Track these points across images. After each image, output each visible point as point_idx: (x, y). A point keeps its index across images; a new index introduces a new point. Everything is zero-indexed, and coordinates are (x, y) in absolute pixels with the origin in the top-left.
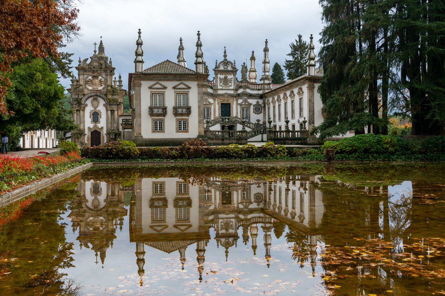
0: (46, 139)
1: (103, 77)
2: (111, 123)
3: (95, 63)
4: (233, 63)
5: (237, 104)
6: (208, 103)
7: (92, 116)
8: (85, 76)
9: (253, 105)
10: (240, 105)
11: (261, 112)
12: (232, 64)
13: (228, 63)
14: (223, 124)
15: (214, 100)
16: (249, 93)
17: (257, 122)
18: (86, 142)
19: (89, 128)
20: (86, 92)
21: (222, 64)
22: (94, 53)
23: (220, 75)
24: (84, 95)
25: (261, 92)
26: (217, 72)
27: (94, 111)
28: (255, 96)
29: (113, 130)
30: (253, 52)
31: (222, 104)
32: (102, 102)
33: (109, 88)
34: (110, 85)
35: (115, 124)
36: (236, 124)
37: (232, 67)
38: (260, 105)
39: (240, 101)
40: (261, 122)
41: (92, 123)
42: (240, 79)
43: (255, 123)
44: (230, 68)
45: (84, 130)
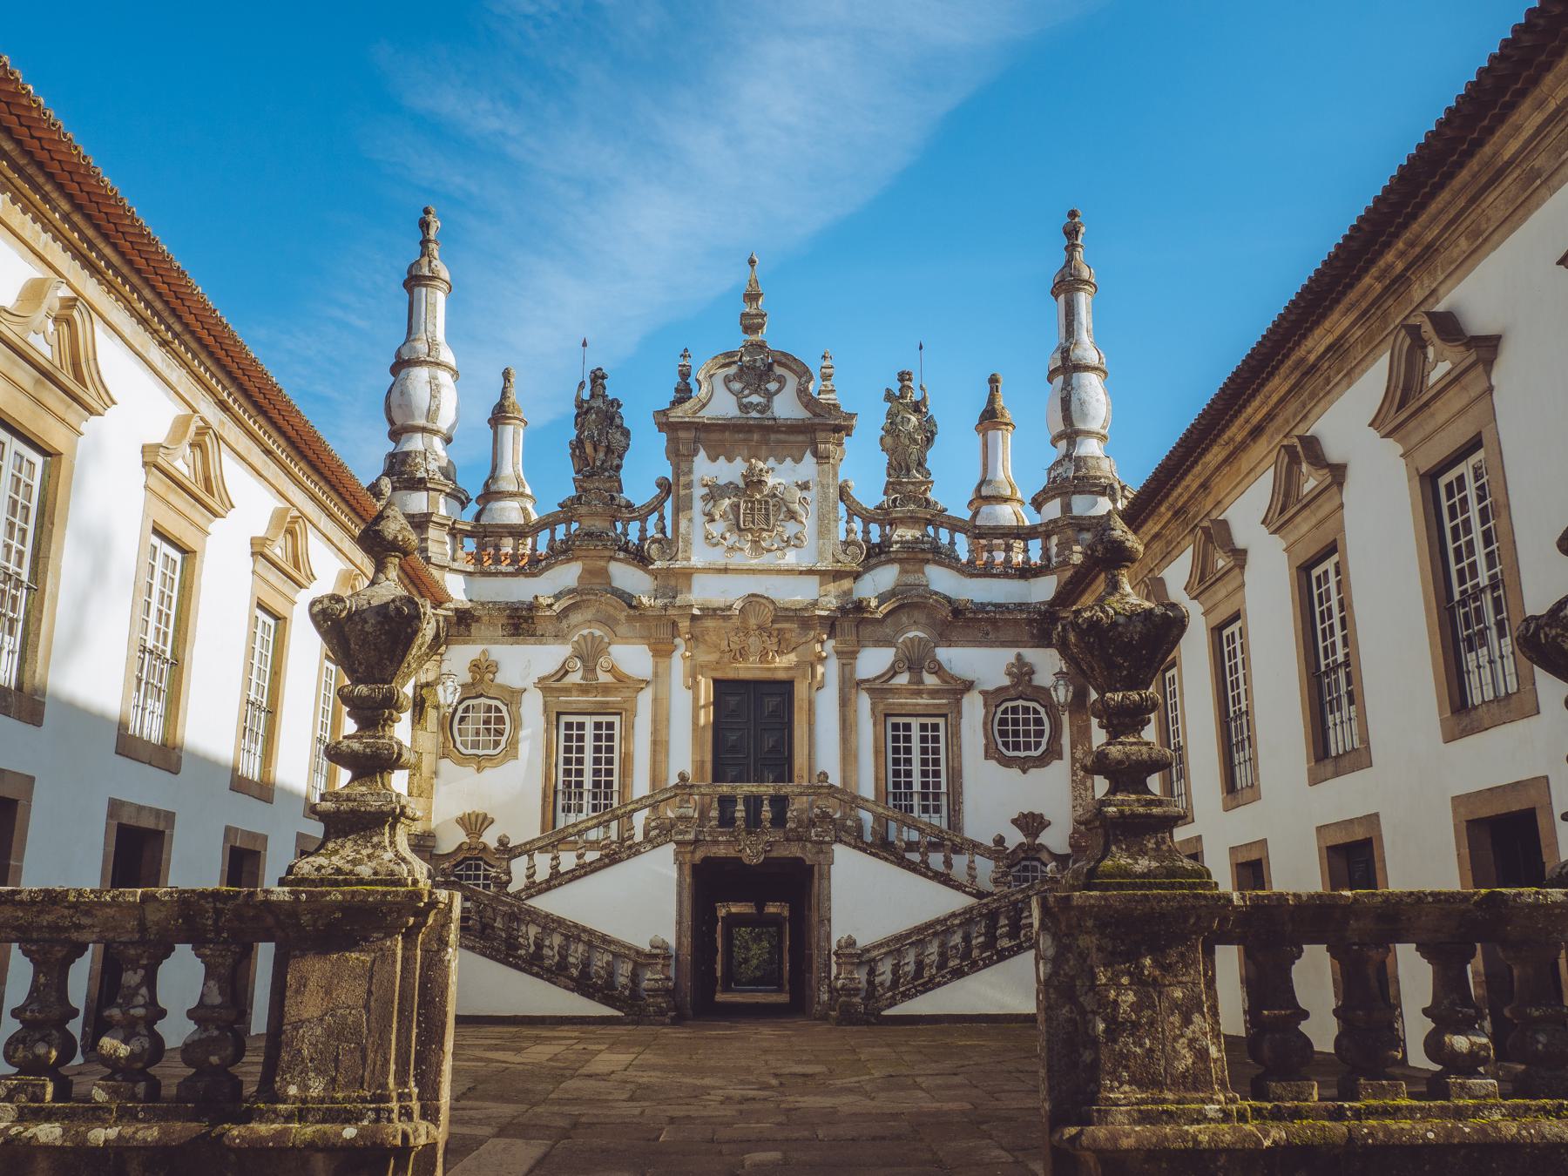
4: (815, 367)
5: (850, 686)
6: (604, 678)
9: (984, 693)
10: (871, 691)
11: (1053, 753)
12: (803, 373)
13: (770, 367)
14: (700, 855)
15: (661, 651)
16: (949, 600)
17: (1015, 838)
21: (727, 380)
23: (713, 459)
25: (1043, 590)
26: (682, 434)
28: (993, 622)
30: (993, 380)
31: (723, 687)
36: (823, 848)
37: (802, 392)
38: (1042, 695)
39: (874, 661)
40: (1056, 839)
42: (870, 492)
43: (1000, 841)
44: (786, 407)
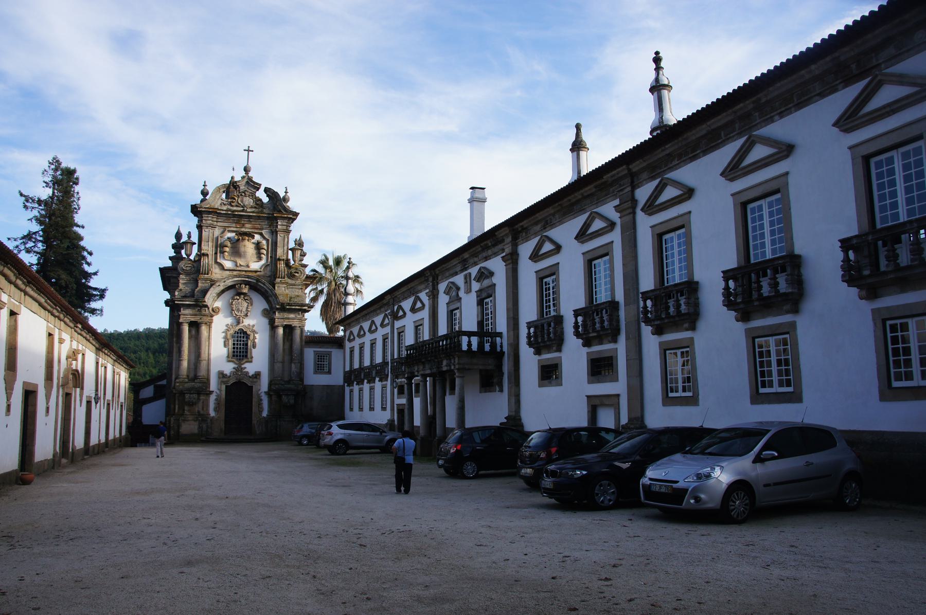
0: (109, 404)
1: (264, 238)
2: (283, 362)
3: (245, 199)
7: (231, 342)
8: (217, 232)
18: (212, 413)
19: (221, 375)
20: (216, 273)
22: (243, 174)
24: (213, 283)
27: (238, 328)
29: (289, 382)
32: (260, 304)
33: (282, 266)
34: (285, 258)
35: (293, 365)
41: (229, 361)
45: (208, 379)
